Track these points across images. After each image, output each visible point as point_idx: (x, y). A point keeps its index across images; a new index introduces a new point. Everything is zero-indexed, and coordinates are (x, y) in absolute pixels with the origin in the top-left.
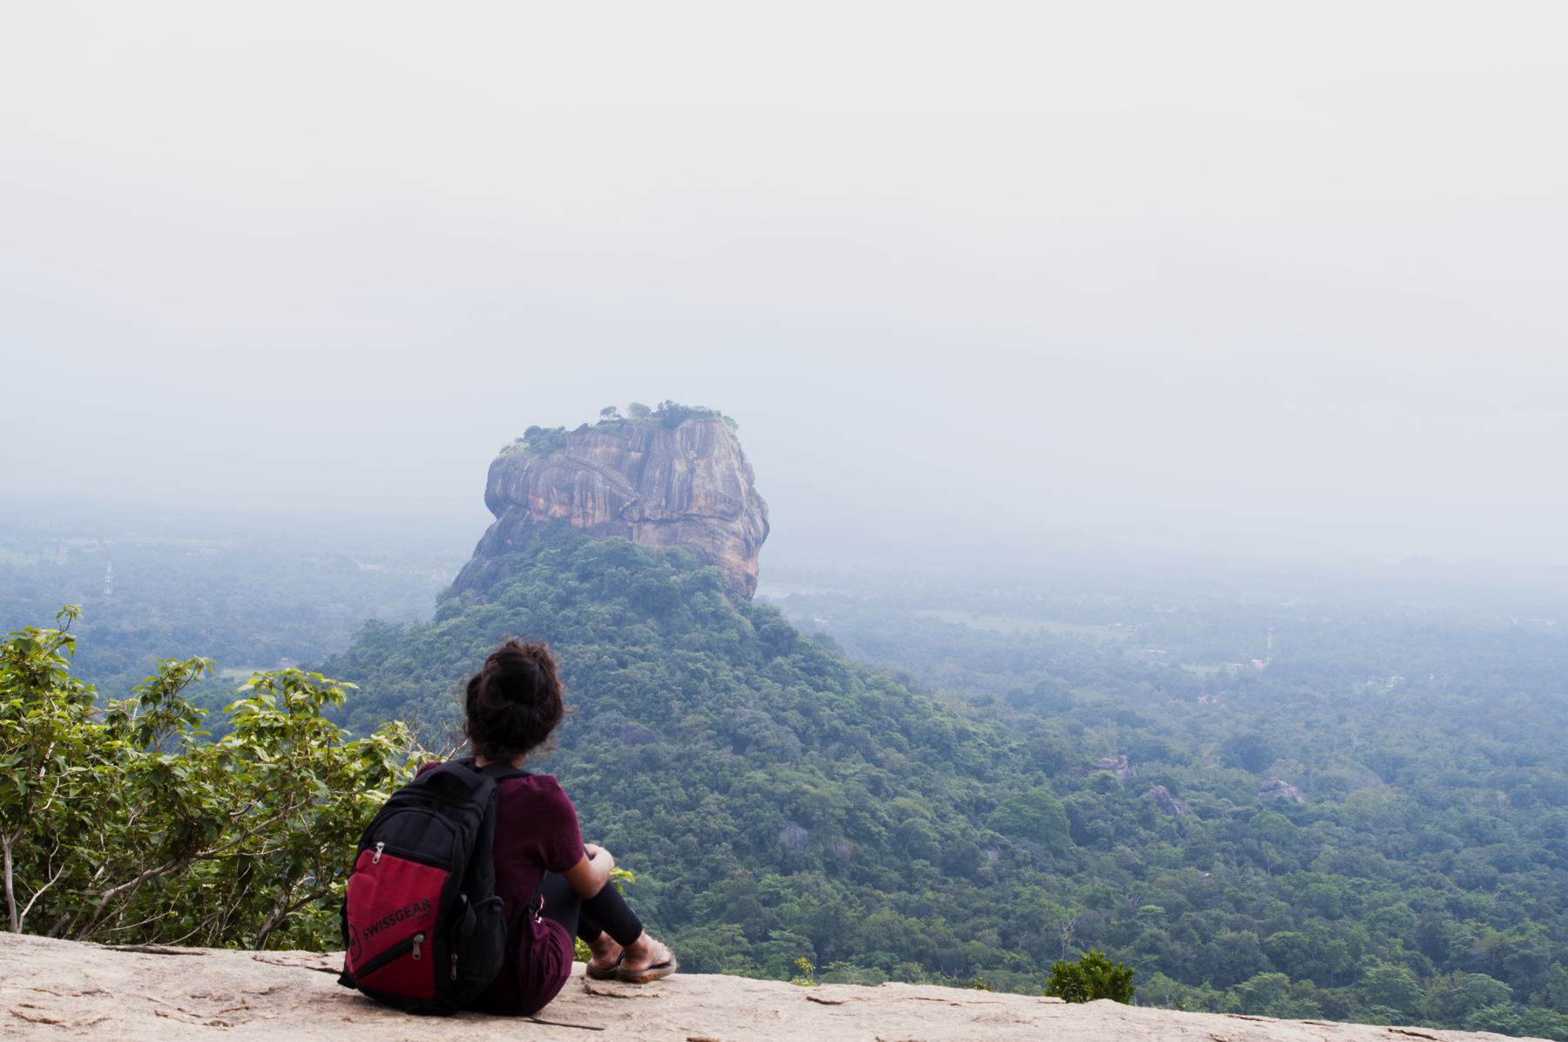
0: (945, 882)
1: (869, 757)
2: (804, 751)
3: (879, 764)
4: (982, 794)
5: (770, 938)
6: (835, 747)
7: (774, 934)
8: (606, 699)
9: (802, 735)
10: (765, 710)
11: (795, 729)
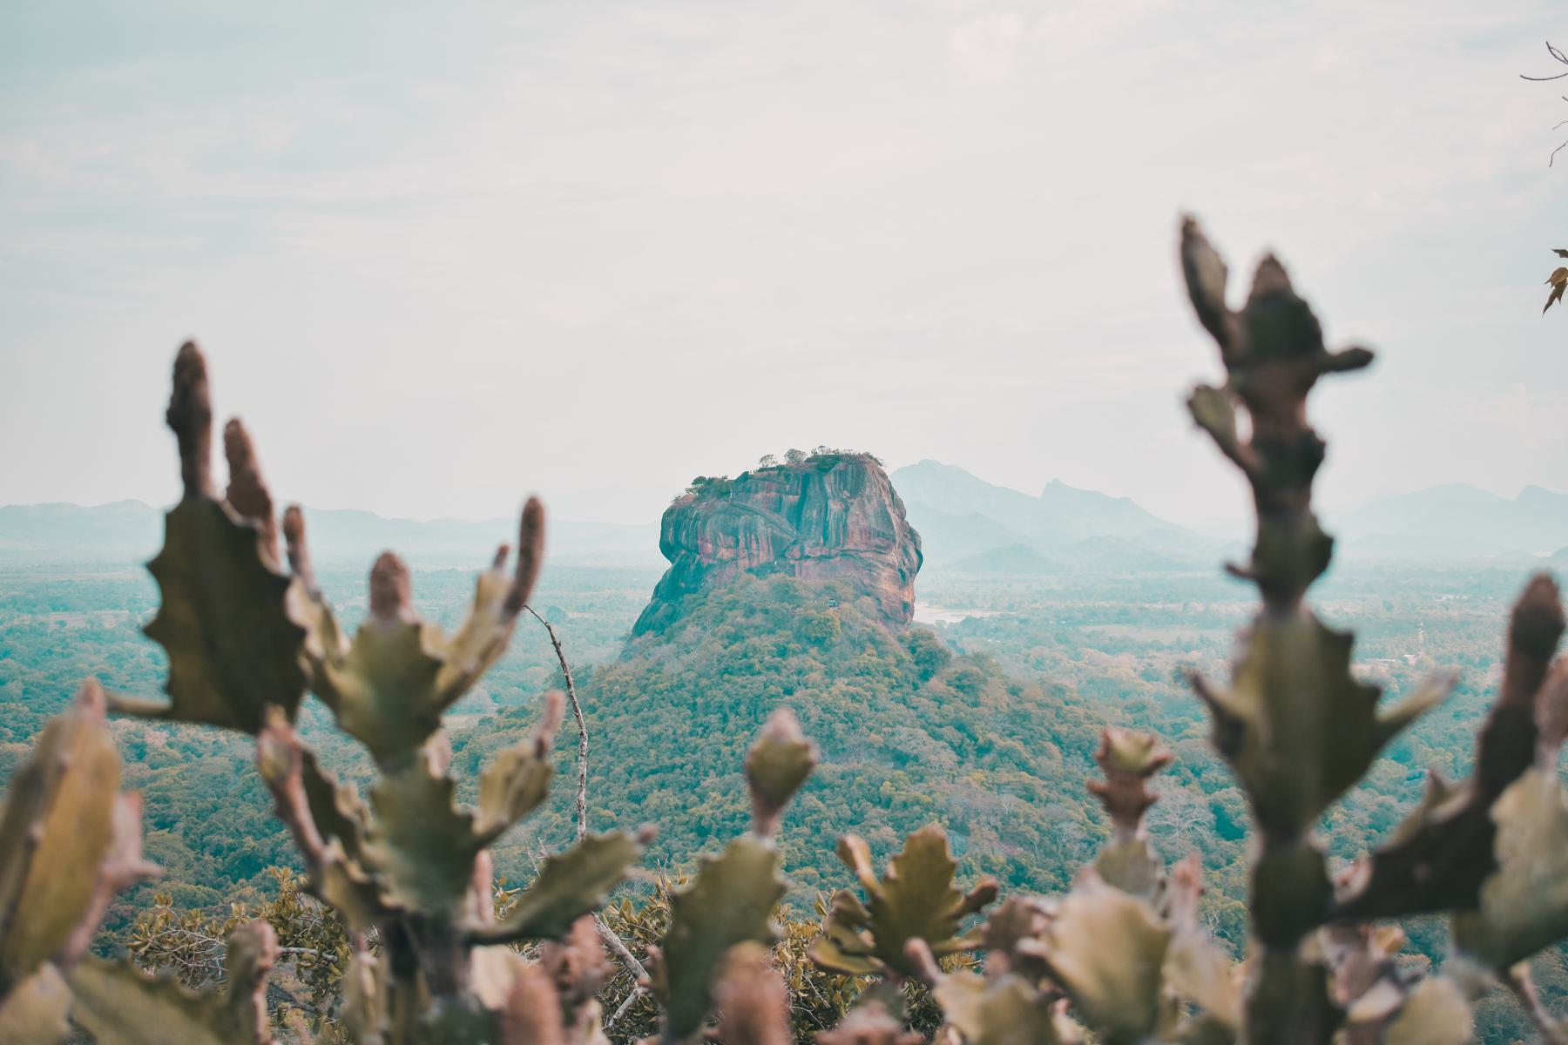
6: (987, 758)
9: (958, 750)
10: (923, 727)
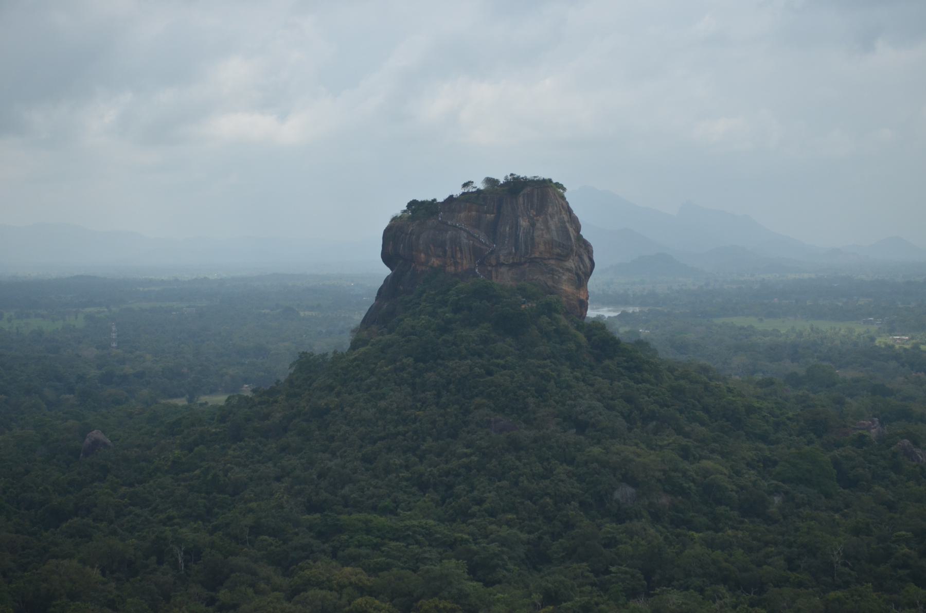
0: (742, 522)
2: (630, 429)
3: (687, 435)
4: (767, 453)
5: (611, 572)
7: (613, 569)
8: (478, 400)
10: (599, 400)
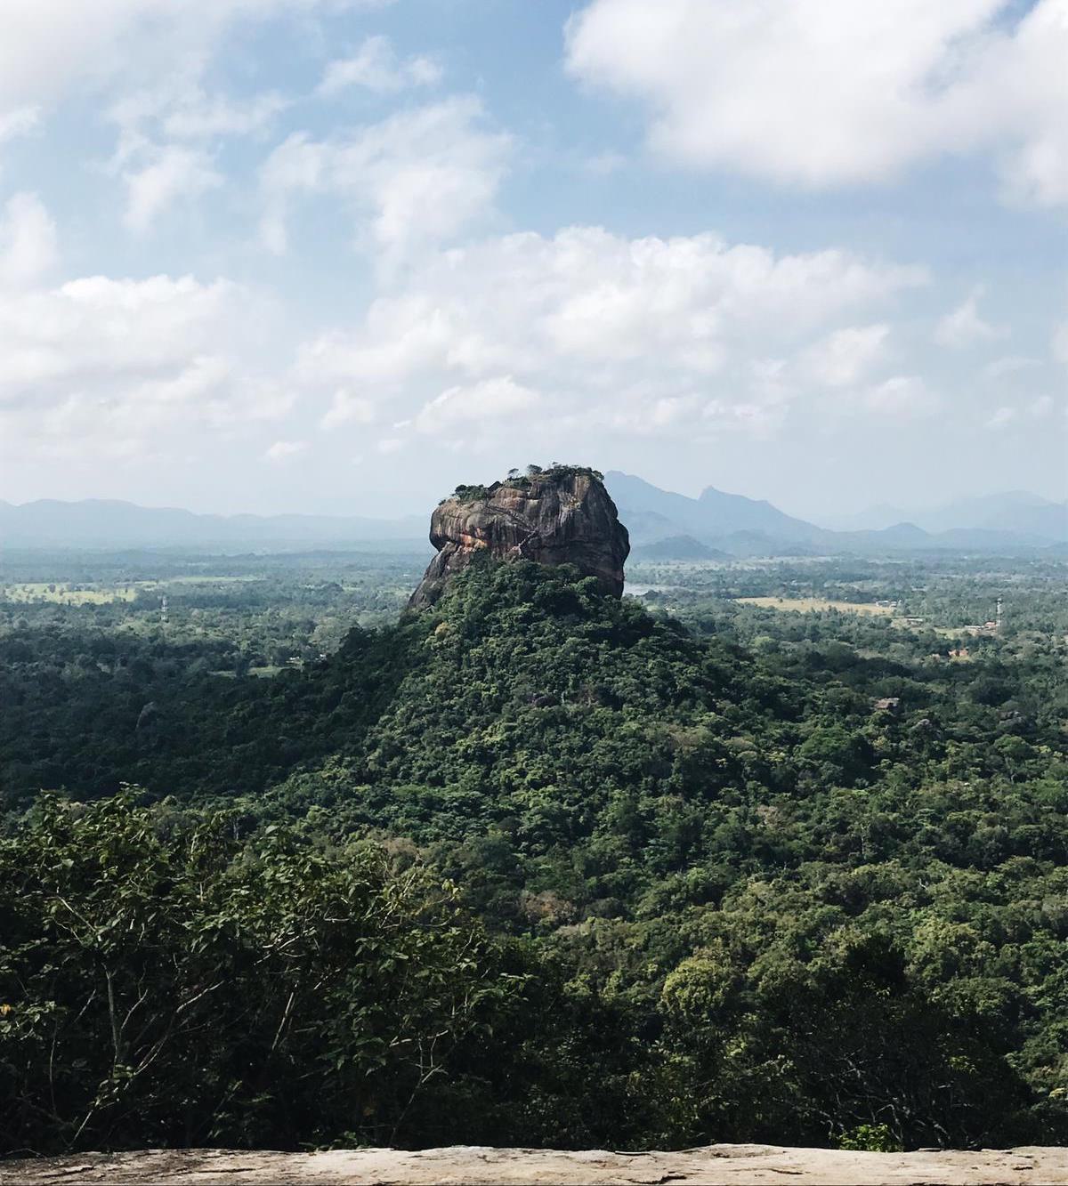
1: (711, 707)
2: (665, 705)
5: (650, 844)
6: (686, 703)
7: (652, 841)
11: (658, 690)
